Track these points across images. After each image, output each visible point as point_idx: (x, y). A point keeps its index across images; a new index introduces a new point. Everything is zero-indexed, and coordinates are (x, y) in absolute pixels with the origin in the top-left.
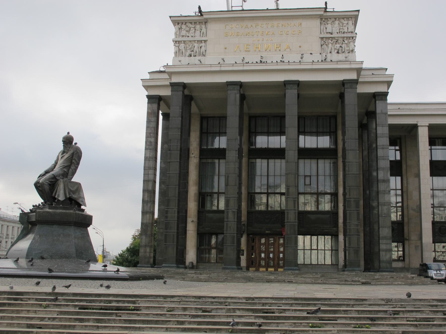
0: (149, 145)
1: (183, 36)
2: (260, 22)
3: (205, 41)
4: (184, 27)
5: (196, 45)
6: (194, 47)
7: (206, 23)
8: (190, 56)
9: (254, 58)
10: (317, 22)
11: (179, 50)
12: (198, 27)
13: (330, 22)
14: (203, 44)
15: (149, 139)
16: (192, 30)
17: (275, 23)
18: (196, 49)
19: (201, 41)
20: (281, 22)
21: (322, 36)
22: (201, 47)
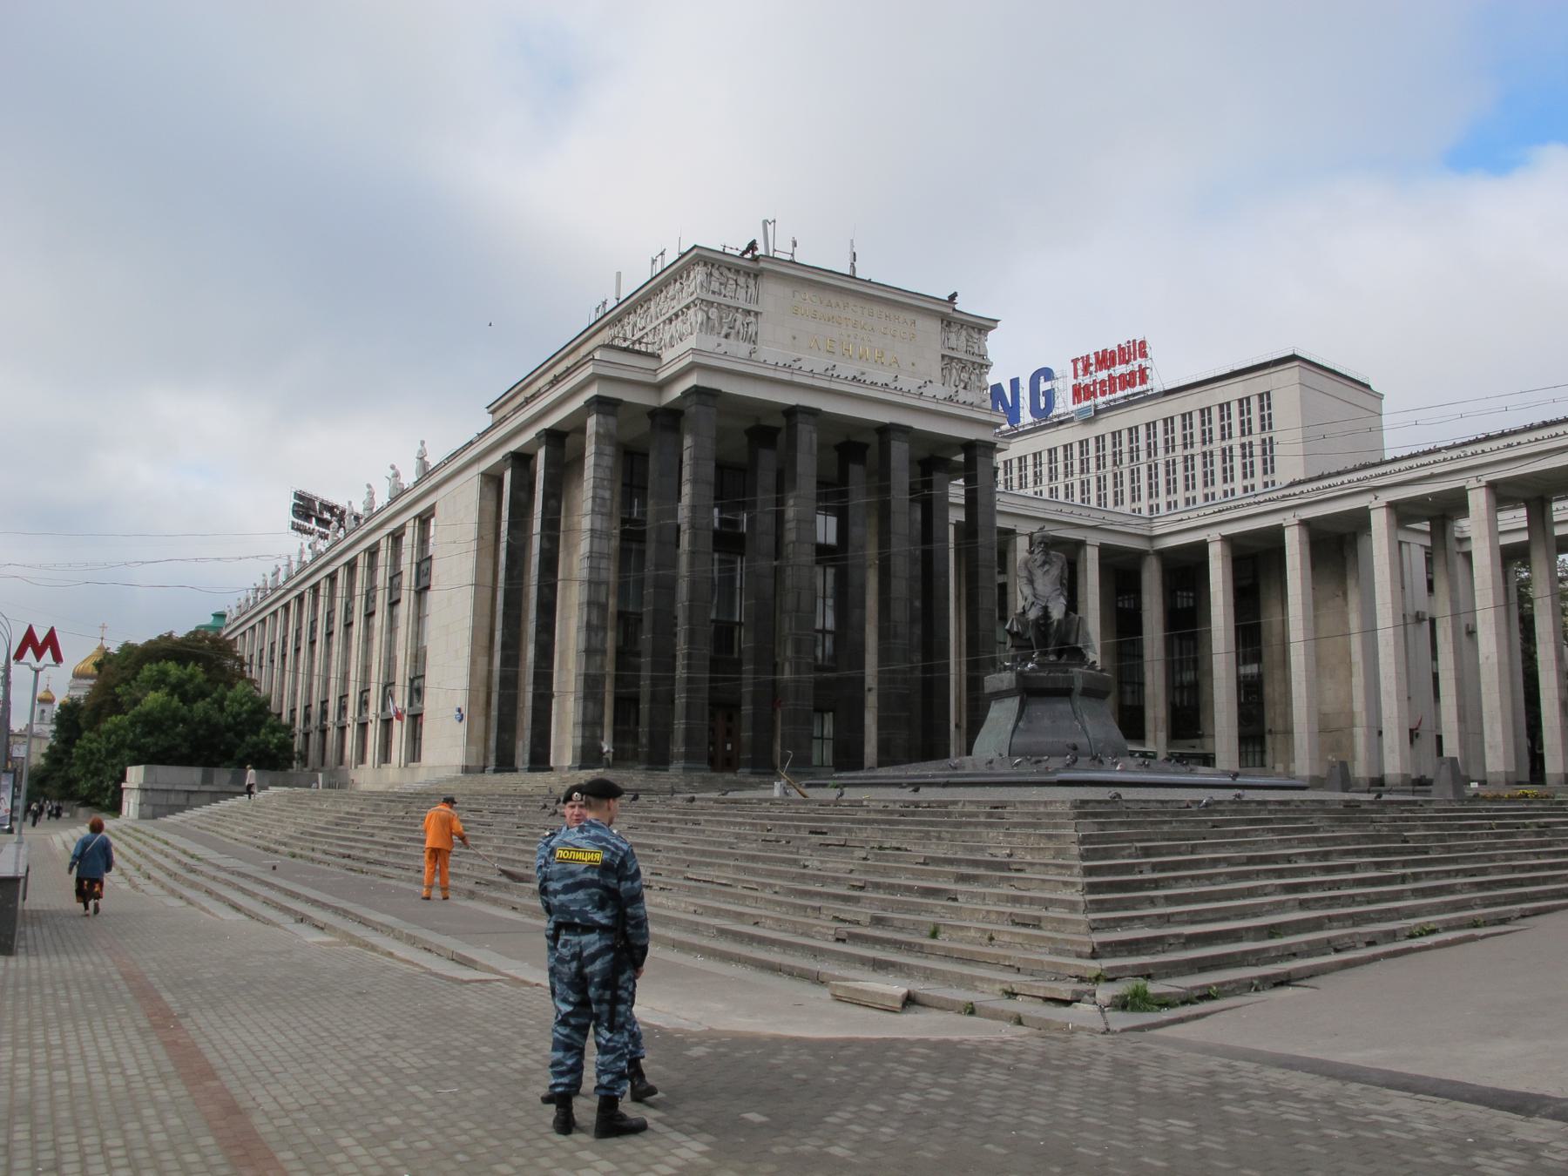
2: (851, 301)
3: (757, 314)
4: (716, 273)
5: (739, 316)
7: (756, 276)
8: (727, 336)
9: (847, 369)
10: (935, 326)
12: (741, 281)
13: (954, 329)
14: (752, 319)
15: (600, 492)
16: (731, 285)
17: (876, 309)
18: (738, 323)
19: (749, 312)
20: (886, 310)
21: (947, 352)
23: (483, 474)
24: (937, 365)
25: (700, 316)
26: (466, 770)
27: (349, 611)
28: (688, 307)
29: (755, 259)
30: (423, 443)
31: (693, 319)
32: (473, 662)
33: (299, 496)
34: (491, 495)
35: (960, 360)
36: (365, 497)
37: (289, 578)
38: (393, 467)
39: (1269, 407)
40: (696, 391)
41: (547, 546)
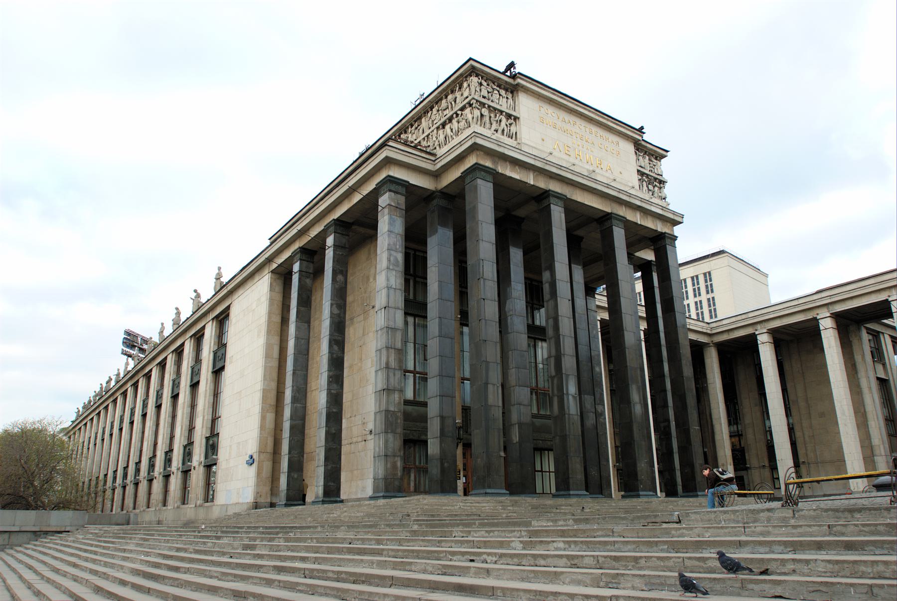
0: (394, 265)
1: (484, 97)
2: (579, 122)
3: (516, 119)
4: (485, 83)
6: (500, 121)
11: (482, 115)
12: (503, 92)
16: (496, 96)
19: (509, 116)
22: (510, 124)
23: (272, 272)
24: (636, 177)
25: (477, 113)
26: (256, 506)
27: (159, 396)
28: (462, 109)
29: (514, 77)
30: (219, 268)
31: (470, 117)
32: (263, 418)
33: (128, 333)
34: (279, 288)
35: (647, 175)
36: (174, 316)
37: (117, 382)
38: (195, 291)
39: (711, 280)
40: (476, 167)
41: (336, 311)
